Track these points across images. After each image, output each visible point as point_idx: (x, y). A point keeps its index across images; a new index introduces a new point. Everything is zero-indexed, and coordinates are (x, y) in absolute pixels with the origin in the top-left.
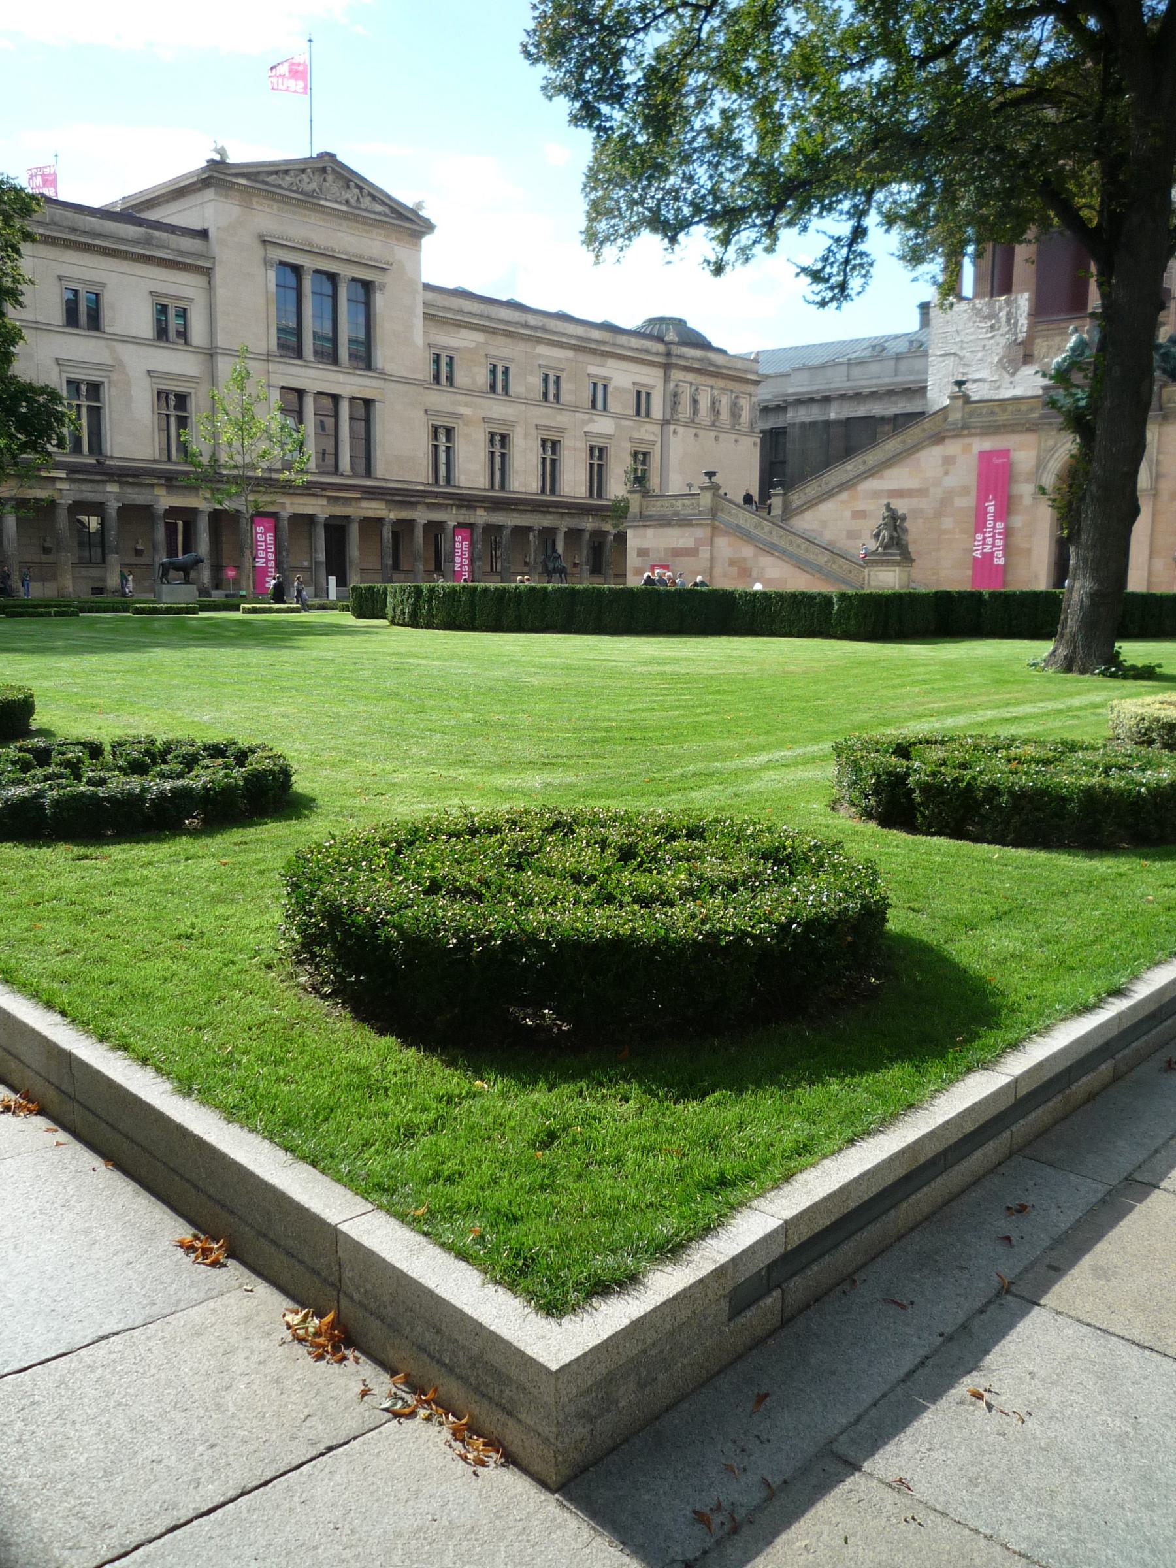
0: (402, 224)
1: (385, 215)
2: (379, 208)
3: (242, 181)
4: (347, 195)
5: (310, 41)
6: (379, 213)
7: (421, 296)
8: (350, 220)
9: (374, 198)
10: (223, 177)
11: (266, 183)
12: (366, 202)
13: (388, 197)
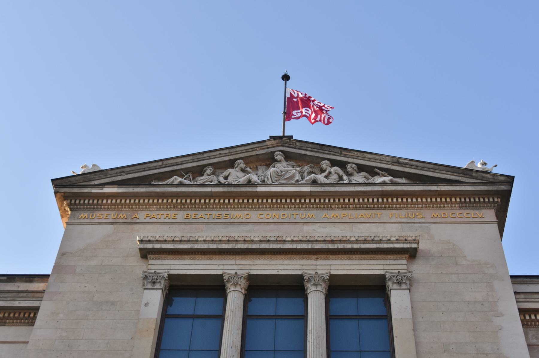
0: (434, 188)
1: (393, 183)
2: (379, 180)
3: (107, 190)
4: (321, 178)
5: (286, 78)
6: (384, 184)
7: (509, 289)
8: (328, 207)
9: (372, 171)
10: (76, 190)
11: (154, 186)
12: (359, 178)
13: (397, 161)
